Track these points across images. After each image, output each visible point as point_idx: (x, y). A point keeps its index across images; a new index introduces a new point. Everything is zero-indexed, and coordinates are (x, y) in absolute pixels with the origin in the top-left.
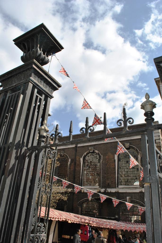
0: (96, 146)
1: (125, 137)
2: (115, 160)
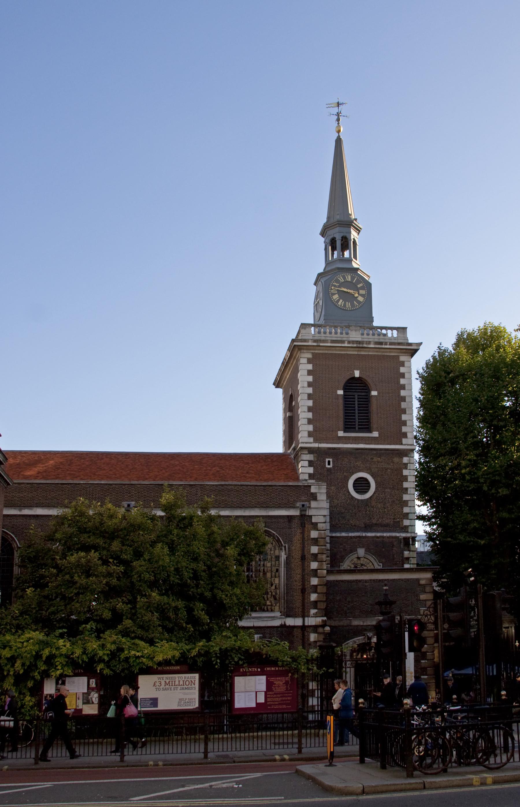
1: (256, 507)
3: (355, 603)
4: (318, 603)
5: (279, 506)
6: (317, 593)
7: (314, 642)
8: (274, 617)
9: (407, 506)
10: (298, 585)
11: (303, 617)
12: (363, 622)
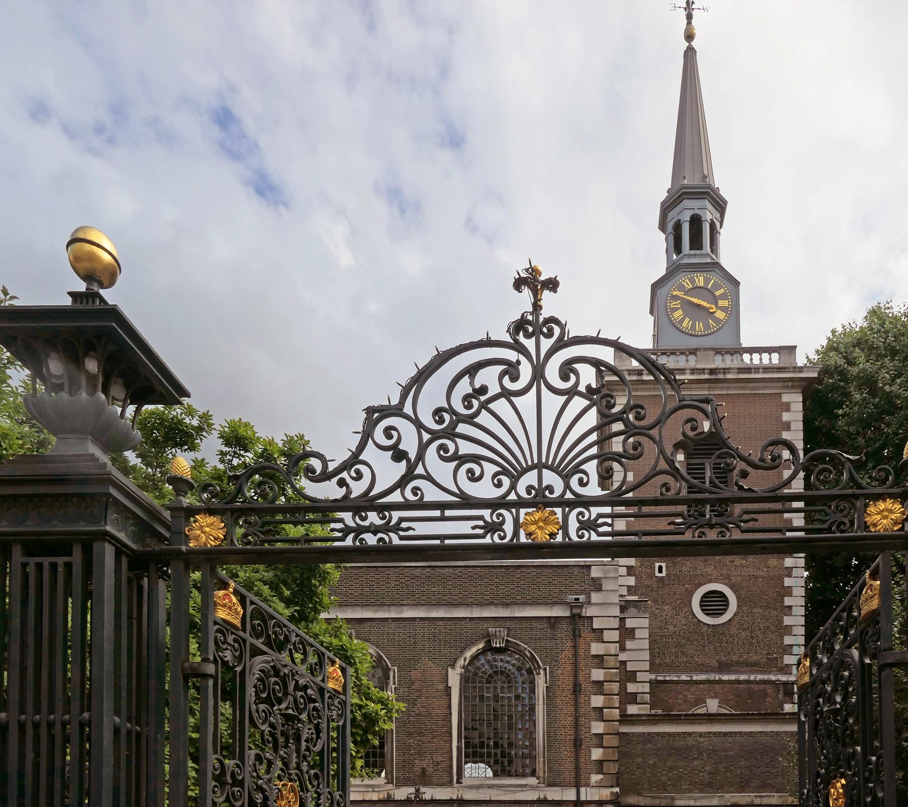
0: (366, 627)
2: (448, 689)
5: (535, 603)
8: (525, 786)
10: (566, 734)
11: (578, 786)
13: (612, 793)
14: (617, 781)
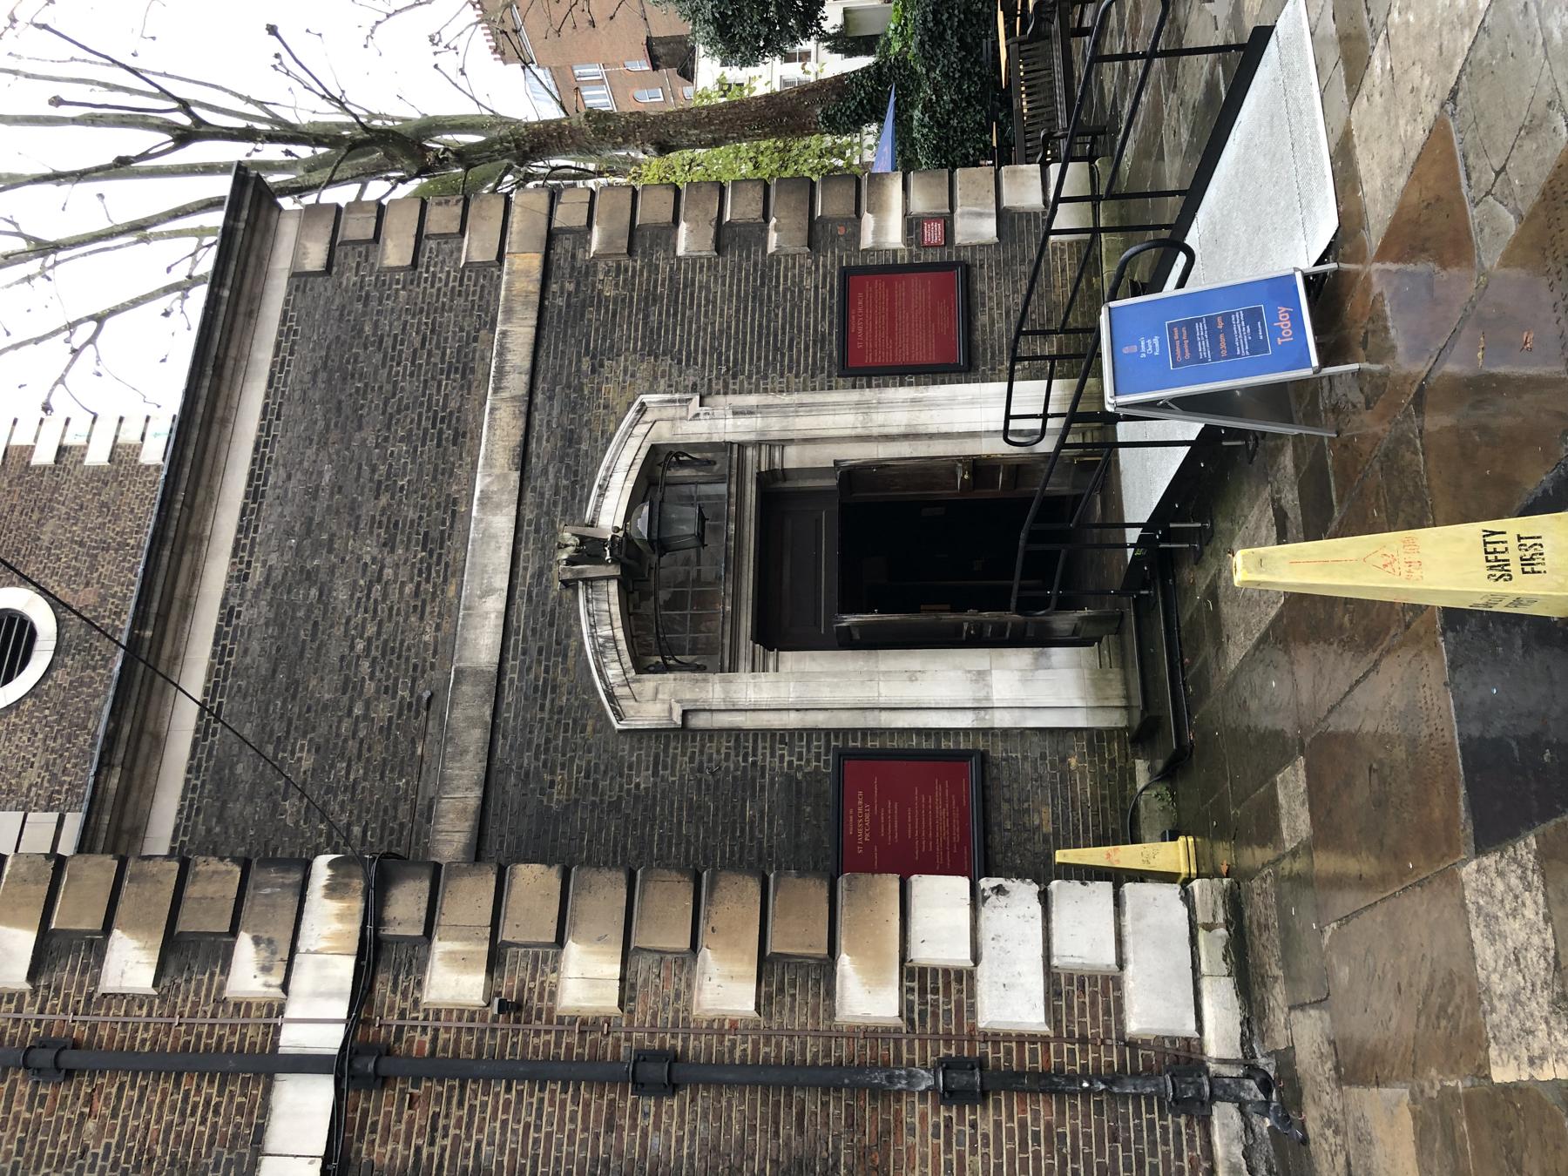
3: (360, 646)
4: (185, 924)
6: (107, 928)
7: (495, 961)
9: (136, 450)
11: (270, 1063)
12: (488, 592)
13: (332, 890)
14: (285, 864)
